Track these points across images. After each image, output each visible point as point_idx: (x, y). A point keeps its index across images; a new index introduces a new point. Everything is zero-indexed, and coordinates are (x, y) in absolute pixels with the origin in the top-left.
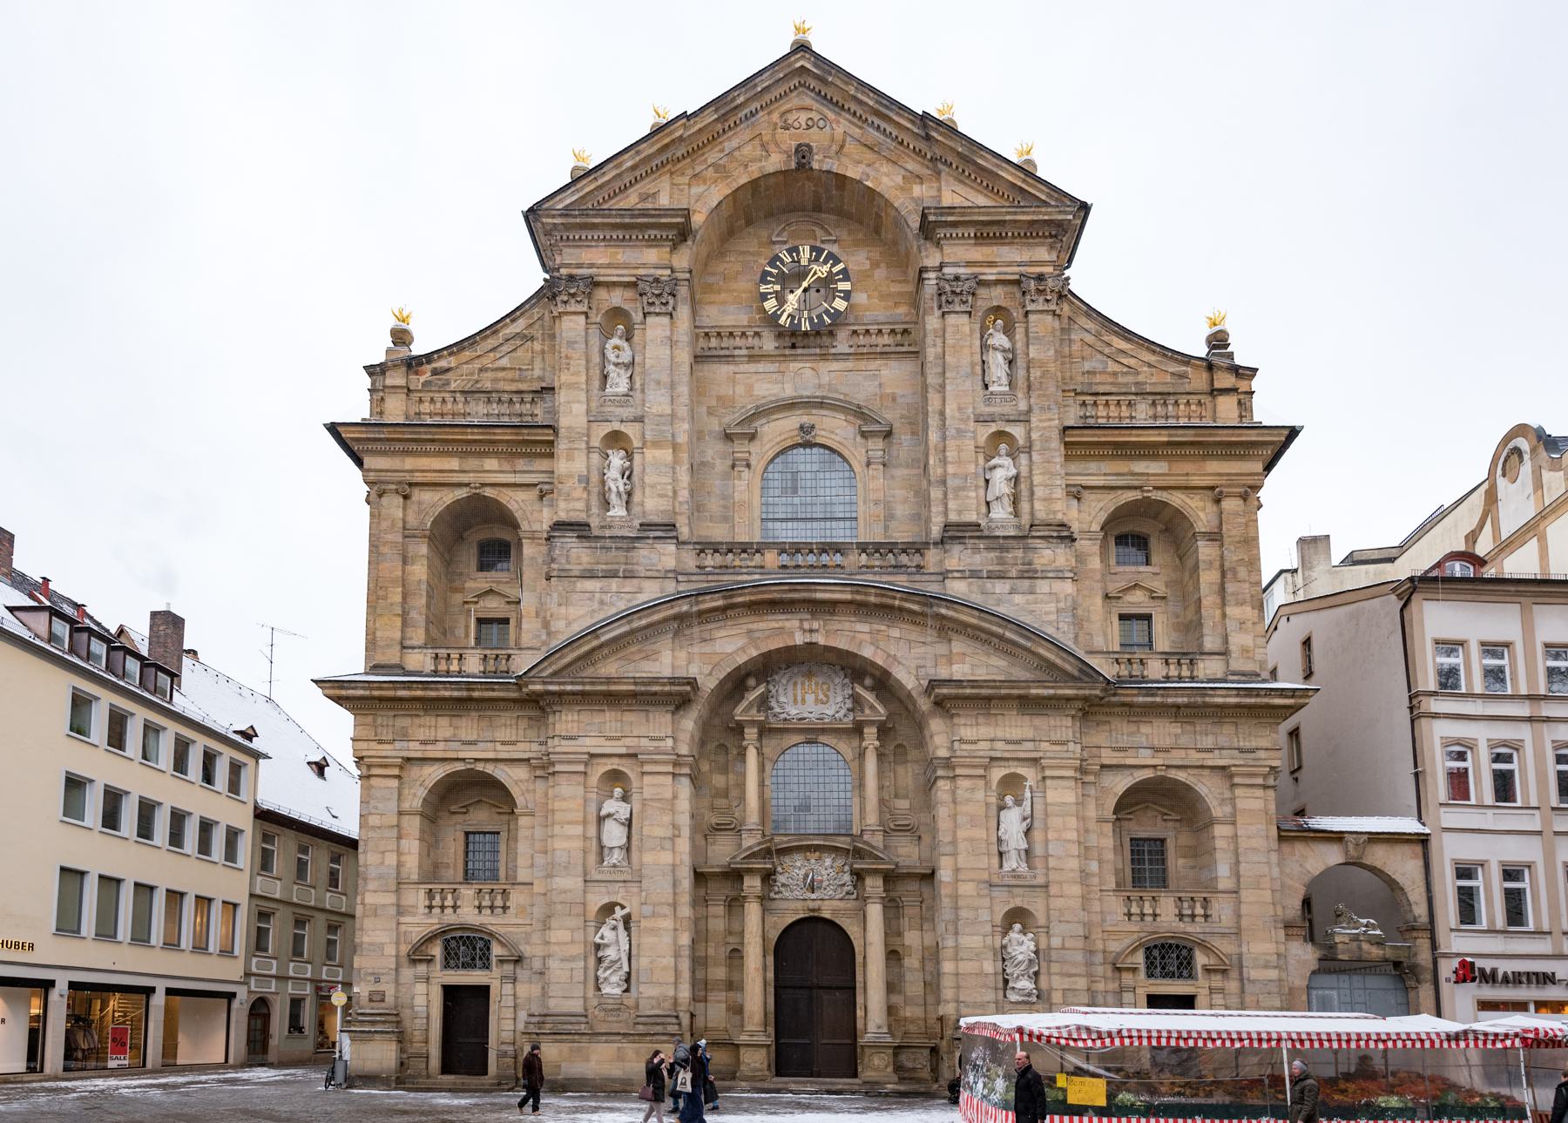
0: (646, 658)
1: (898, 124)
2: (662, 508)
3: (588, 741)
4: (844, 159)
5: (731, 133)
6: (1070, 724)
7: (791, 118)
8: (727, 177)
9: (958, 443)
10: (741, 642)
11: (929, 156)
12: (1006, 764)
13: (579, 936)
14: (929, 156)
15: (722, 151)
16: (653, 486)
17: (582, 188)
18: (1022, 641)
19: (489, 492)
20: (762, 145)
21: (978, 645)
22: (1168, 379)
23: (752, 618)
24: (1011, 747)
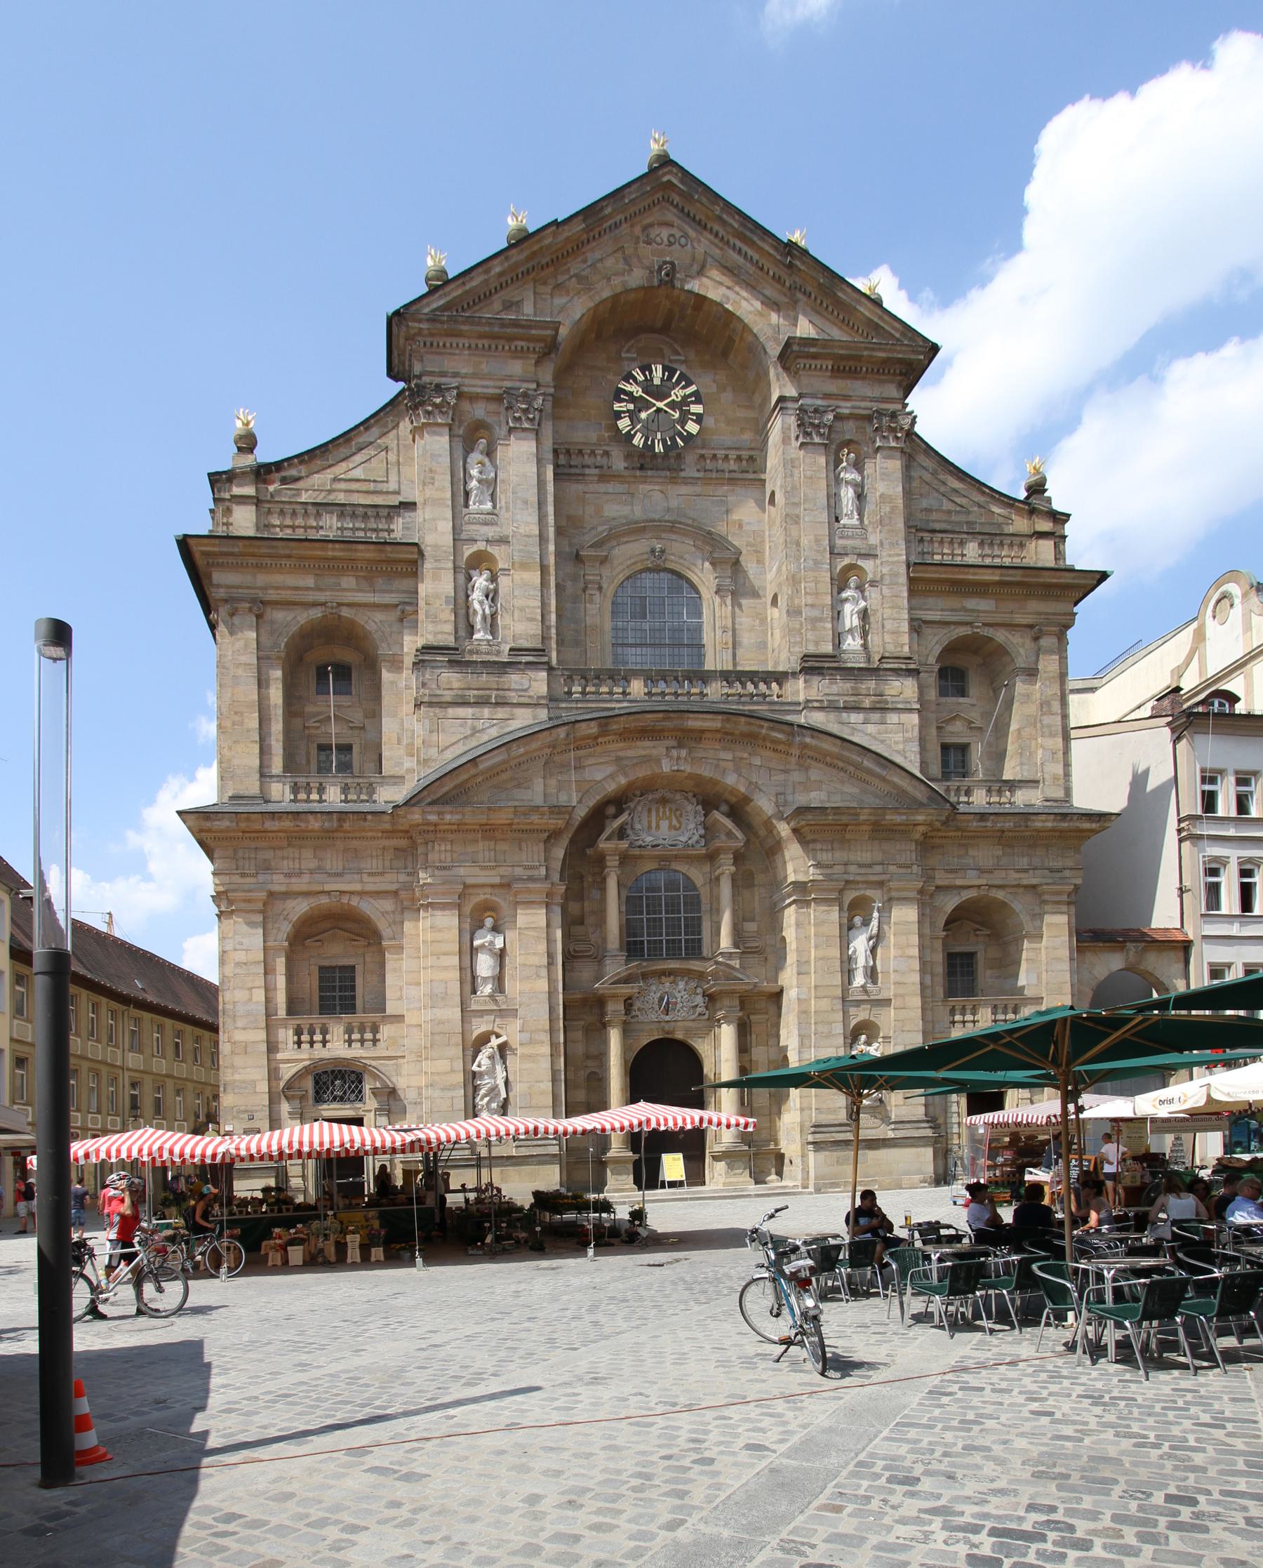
0: (519, 786)
1: (760, 249)
2: (532, 632)
3: (462, 871)
4: (705, 280)
5: (594, 244)
6: (913, 848)
7: (654, 232)
8: (590, 290)
9: (816, 574)
10: (610, 769)
11: (787, 284)
13: (459, 1065)
14: (787, 284)
15: (585, 261)
16: (522, 609)
17: (450, 293)
18: (878, 770)
19: (346, 612)
20: (625, 259)
21: (835, 771)
23: (622, 744)
24: (863, 871)
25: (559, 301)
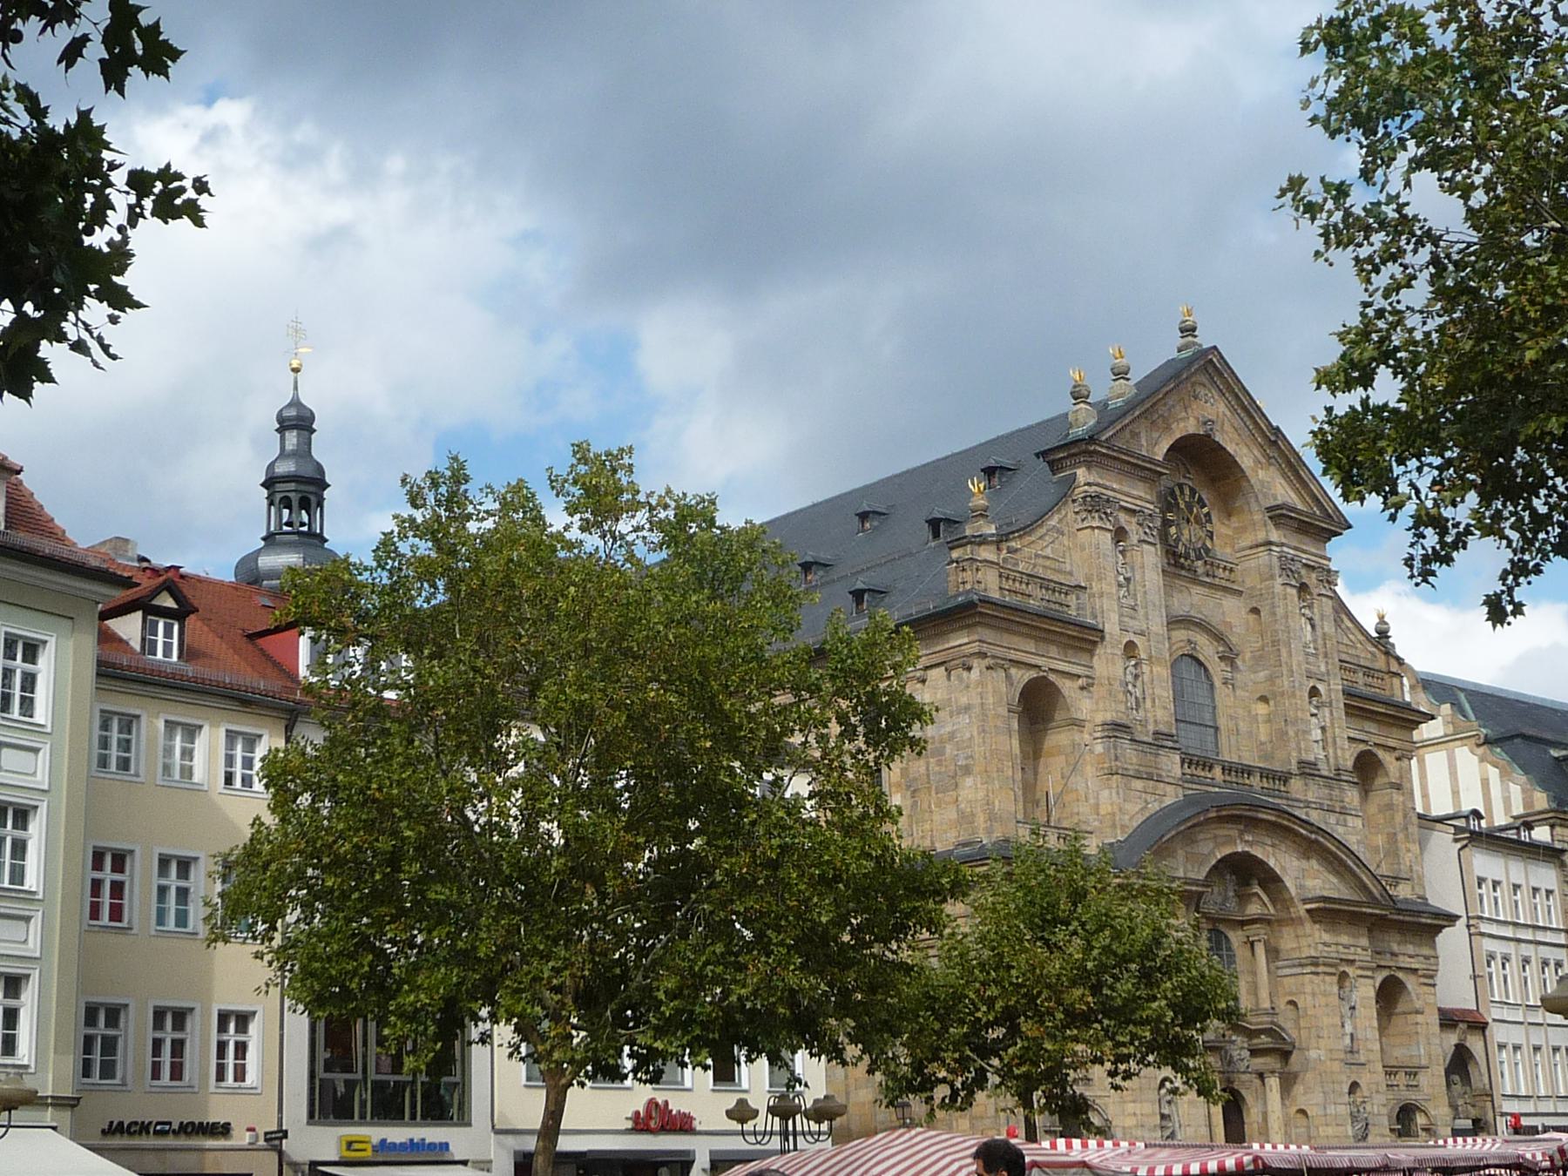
22: (1369, 656)
25: (1155, 435)
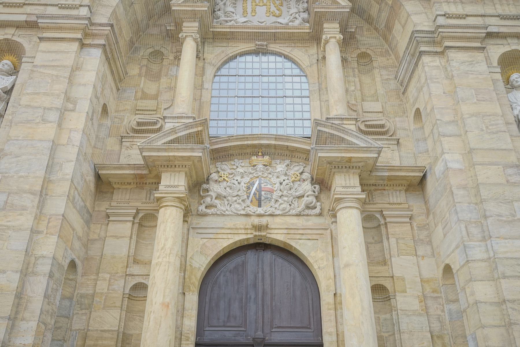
12: (504, 41)
